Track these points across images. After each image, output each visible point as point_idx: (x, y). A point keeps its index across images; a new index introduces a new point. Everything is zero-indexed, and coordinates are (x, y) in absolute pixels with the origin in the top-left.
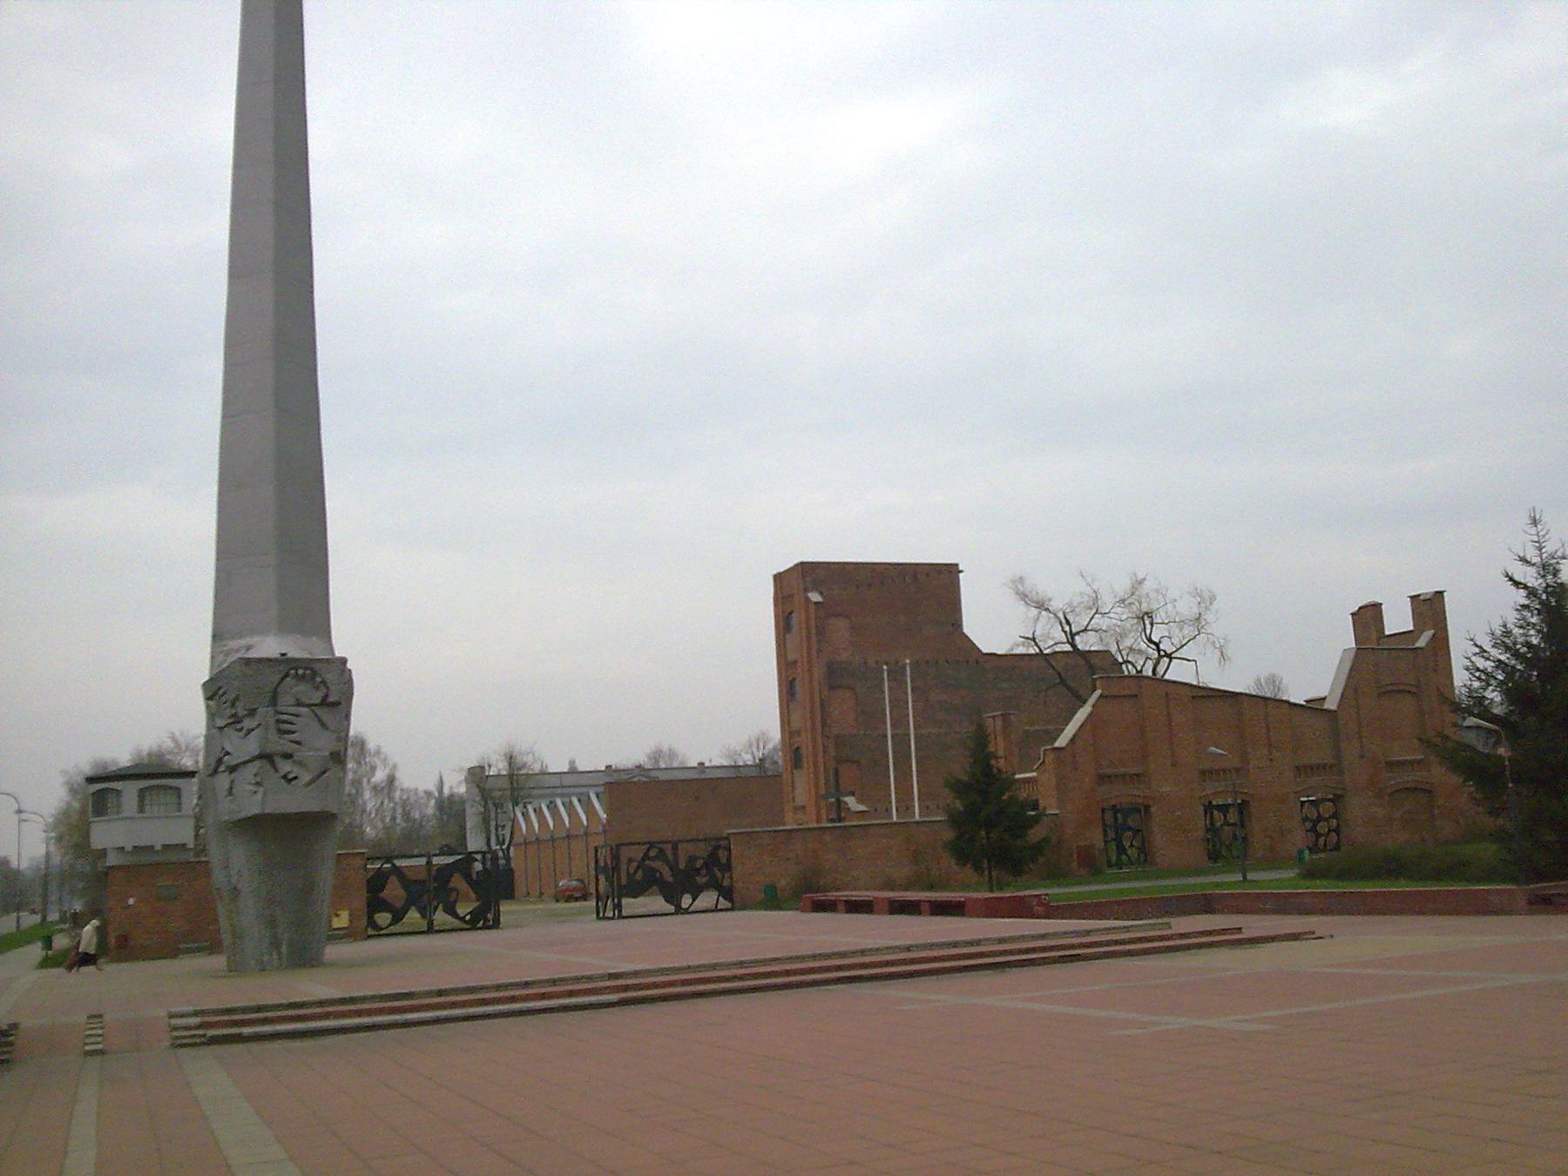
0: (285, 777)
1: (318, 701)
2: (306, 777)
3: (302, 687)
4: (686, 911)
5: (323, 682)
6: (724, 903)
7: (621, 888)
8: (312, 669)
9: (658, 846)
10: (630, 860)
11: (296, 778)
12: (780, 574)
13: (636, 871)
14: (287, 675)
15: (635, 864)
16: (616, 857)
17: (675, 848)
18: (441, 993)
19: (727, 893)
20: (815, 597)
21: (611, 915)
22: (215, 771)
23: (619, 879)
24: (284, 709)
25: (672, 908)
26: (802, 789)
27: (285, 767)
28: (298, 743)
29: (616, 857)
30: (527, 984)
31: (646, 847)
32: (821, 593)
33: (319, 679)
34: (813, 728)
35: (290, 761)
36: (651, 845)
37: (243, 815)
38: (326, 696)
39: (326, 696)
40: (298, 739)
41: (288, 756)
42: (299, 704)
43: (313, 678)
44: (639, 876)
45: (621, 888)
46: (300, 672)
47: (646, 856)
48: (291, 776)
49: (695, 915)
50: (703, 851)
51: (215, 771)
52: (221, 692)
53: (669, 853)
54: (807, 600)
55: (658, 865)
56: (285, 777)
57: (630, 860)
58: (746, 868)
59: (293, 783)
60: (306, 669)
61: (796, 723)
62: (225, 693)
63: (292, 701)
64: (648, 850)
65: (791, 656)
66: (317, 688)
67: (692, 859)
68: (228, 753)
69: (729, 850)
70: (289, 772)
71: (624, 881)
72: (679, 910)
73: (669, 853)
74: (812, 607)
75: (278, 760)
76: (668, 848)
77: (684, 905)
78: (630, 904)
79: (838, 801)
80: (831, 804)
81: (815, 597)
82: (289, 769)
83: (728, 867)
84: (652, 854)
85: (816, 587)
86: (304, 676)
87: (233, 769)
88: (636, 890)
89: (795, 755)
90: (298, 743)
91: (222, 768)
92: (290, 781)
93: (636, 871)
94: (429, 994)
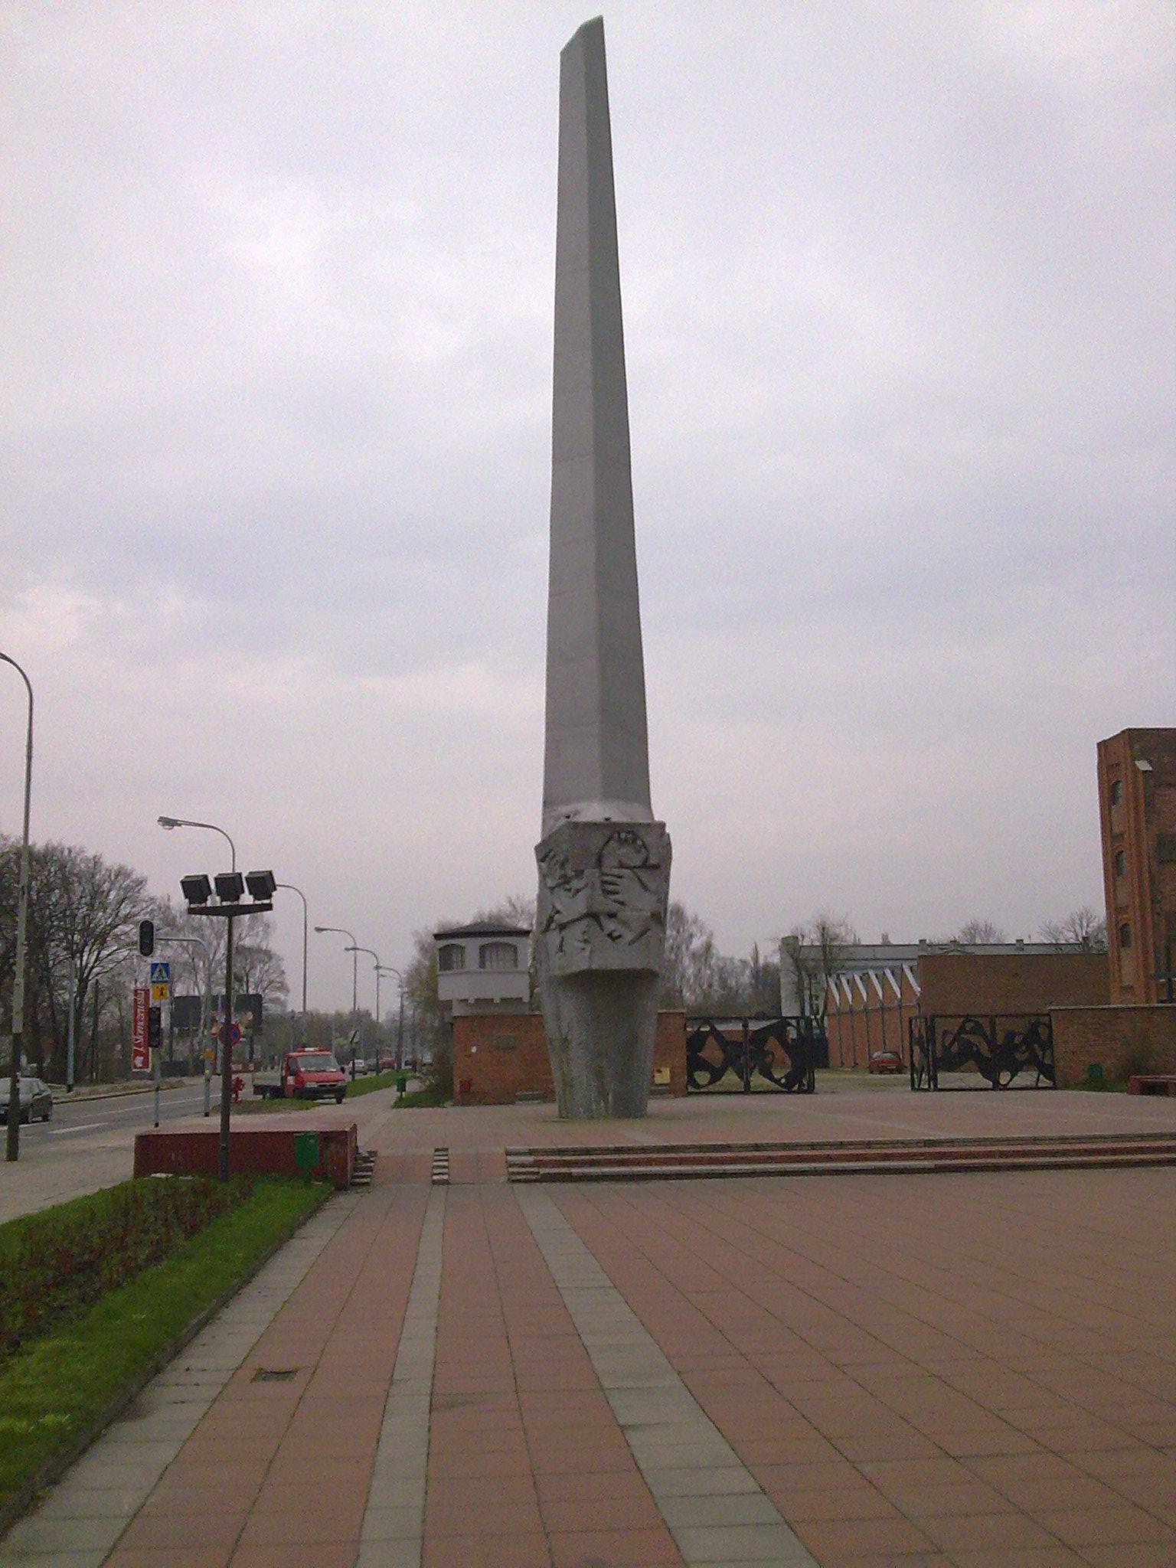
1: (638, 863)
2: (629, 936)
3: (624, 850)
4: (1005, 1088)
5: (644, 846)
6: (1045, 1082)
7: (936, 1060)
8: (633, 833)
9: (979, 1019)
10: (945, 1033)
11: (620, 936)
12: (1104, 741)
13: (951, 1045)
14: (611, 838)
15: (949, 1039)
16: (931, 1029)
17: (993, 1025)
18: (757, 1147)
19: (1047, 1071)
20: (1143, 766)
21: (927, 1087)
22: (547, 929)
23: (934, 1052)
25: (990, 1084)
26: (1129, 968)
27: (610, 925)
28: (622, 903)
29: (931, 1029)
30: (841, 1145)
31: (962, 1020)
32: (1150, 762)
33: (639, 843)
34: (1142, 906)
36: (968, 1018)
37: (569, 971)
38: (647, 859)
39: (647, 859)
40: (621, 900)
41: (612, 915)
42: (622, 866)
43: (634, 841)
44: (955, 1048)
45: (936, 1060)
46: (623, 835)
47: (962, 1030)
48: (615, 934)
49: (1013, 1093)
50: (1020, 1026)
51: (547, 929)
52: (552, 854)
53: (987, 1030)
54: (1135, 769)
55: (973, 1039)
56: (610, 935)
57: (945, 1033)
58: (1067, 1044)
59: (618, 940)
60: (629, 833)
61: (1123, 898)
62: (554, 856)
64: (964, 1023)
65: (1117, 830)
66: (639, 852)
67: (1011, 1035)
68: (558, 912)
69: (1050, 1027)
70: (614, 931)
71: (939, 1054)
72: (997, 1086)
73: (987, 1030)
74: (1140, 777)
76: (986, 1024)
77: (1003, 1082)
78: (945, 1078)
79: (1170, 980)
80: (1163, 985)
81: (1143, 766)
82: (613, 928)
83: (1049, 1044)
84: (969, 1026)
85: (1144, 755)
87: (562, 927)
88: (953, 1063)
89: (1120, 931)
91: (553, 926)
93: (951, 1045)
94: (746, 1148)
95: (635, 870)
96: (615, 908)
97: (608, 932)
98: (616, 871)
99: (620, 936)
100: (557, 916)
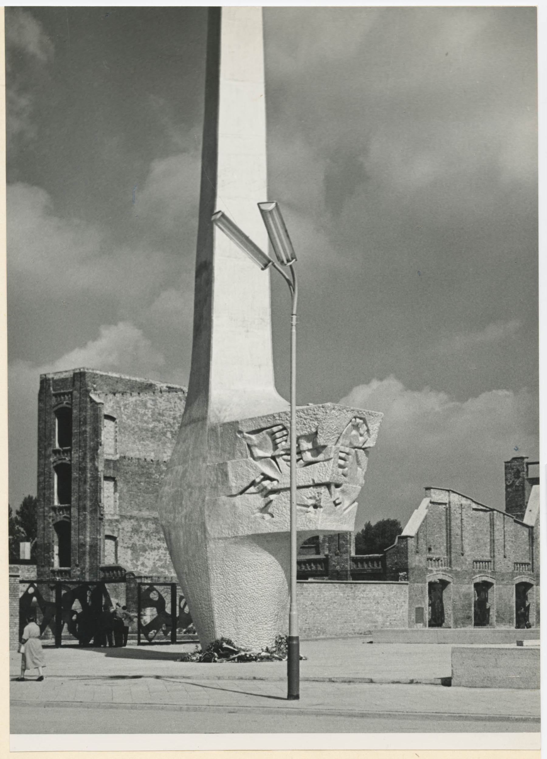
0: (334, 502)
2: (347, 503)
3: (354, 432)
5: (368, 431)
11: (339, 504)
13: (184, 606)
24: (342, 448)
27: (337, 493)
35: (339, 489)
41: (337, 486)
48: (337, 502)
56: (334, 502)
59: (338, 507)
60: (361, 418)
63: (348, 442)
66: (361, 435)
68: (266, 478)
70: (338, 499)
75: (333, 487)
86: (358, 425)
90: (345, 475)
92: (336, 505)
93: (184, 606)
95: (356, 449)
96: (341, 479)
97: (333, 499)
98: (347, 450)
99: (339, 504)
100: (266, 483)
